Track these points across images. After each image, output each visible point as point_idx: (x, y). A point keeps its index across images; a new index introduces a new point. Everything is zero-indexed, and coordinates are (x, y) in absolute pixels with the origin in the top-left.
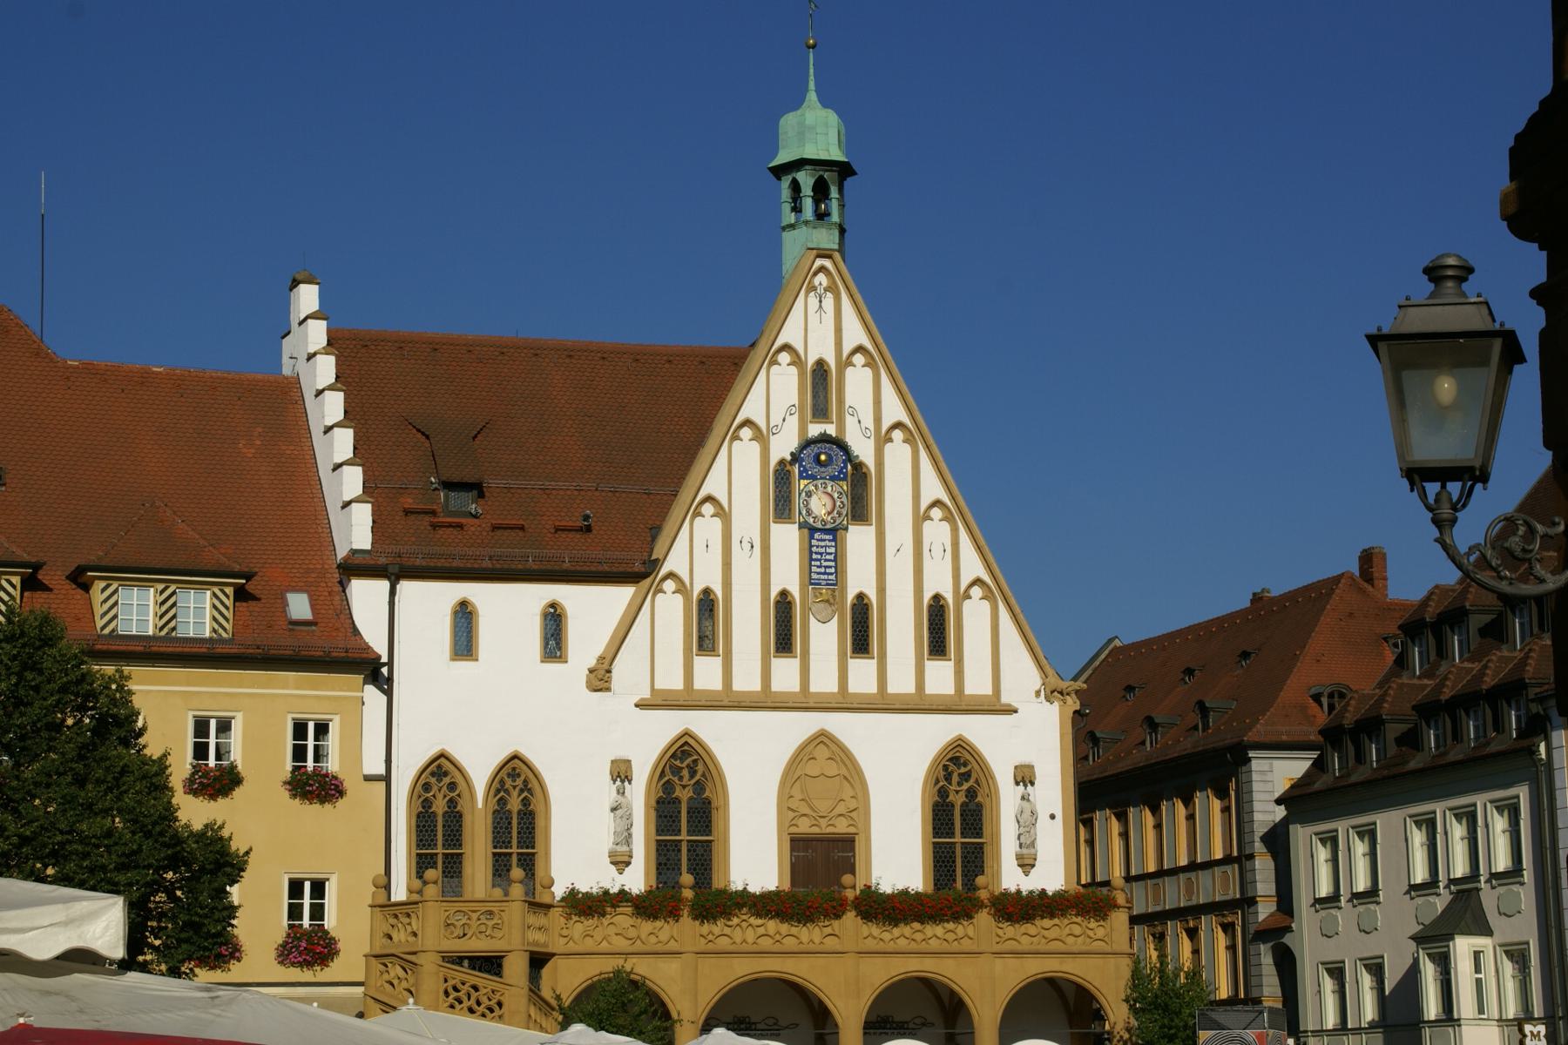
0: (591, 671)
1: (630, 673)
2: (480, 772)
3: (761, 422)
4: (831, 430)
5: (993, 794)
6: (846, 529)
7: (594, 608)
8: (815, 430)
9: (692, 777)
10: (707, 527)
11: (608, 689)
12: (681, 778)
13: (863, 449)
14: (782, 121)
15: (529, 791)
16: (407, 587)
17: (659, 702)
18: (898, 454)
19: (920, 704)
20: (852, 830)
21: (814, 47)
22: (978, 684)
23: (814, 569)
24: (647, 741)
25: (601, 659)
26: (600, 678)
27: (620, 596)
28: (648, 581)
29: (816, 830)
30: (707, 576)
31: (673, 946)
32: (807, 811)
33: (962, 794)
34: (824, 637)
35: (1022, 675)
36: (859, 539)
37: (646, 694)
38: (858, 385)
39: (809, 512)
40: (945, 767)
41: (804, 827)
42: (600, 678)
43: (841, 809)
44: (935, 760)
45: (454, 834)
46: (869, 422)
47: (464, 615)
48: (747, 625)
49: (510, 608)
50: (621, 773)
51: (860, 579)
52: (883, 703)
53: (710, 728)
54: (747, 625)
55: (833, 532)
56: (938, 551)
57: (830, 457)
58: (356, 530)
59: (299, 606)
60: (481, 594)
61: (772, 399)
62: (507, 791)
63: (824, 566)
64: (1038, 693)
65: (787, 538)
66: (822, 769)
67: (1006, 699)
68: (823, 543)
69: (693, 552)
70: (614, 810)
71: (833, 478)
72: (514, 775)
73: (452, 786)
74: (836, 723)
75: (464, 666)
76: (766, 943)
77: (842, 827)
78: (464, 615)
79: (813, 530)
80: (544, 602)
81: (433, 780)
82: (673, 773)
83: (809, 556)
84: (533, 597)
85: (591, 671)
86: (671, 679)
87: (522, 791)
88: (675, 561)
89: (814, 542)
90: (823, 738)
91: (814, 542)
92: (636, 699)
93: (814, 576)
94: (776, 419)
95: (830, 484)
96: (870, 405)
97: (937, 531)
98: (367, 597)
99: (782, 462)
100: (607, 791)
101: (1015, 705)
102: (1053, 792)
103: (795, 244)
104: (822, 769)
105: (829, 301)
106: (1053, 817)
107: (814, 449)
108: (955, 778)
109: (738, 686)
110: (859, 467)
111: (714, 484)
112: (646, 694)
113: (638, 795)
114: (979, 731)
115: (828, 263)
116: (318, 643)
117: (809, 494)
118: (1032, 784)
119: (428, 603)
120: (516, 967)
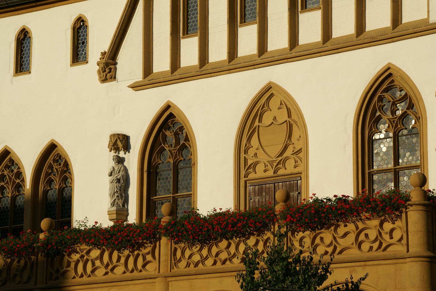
24: (137, 115)
26: (109, 68)
37: (139, 76)
47: (23, 39)
50: (121, 143)
60: (34, 20)
66: (268, 120)
75: (23, 78)
77: (290, 168)
78: (23, 39)
90: (268, 92)
92: (131, 82)
104: (268, 120)
113: (133, 161)
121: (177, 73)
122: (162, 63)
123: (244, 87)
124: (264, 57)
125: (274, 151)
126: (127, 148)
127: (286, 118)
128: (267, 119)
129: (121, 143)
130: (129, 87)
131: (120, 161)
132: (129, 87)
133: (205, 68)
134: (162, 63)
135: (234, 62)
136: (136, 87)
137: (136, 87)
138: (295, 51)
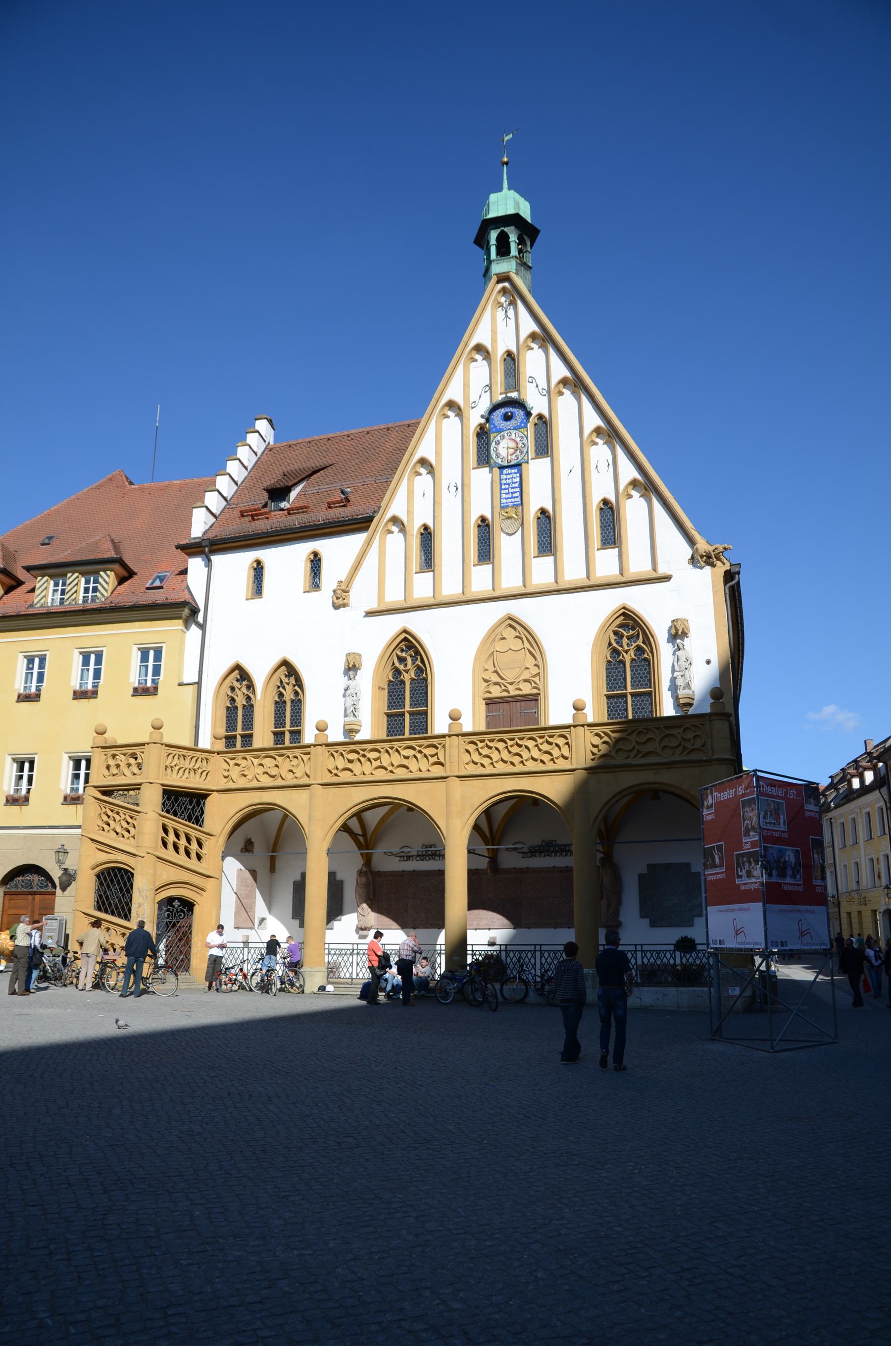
1: (363, 595)
3: (460, 401)
4: (514, 395)
6: (527, 462)
7: (338, 551)
8: (500, 398)
10: (424, 481)
13: (537, 404)
16: (216, 559)
18: (567, 402)
20: (535, 691)
22: (639, 564)
23: (503, 496)
27: (357, 540)
29: (505, 694)
30: (422, 516)
31: (305, 780)
32: (498, 680)
33: (632, 653)
34: (508, 547)
35: (674, 549)
36: (537, 471)
38: (534, 362)
39: (498, 456)
40: (616, 633)
41: (496, 692)
43: (526, 675)
44: (605, 628)
45: (249, 723)
46: (543, 384)
48: (451, 546)
51: (538, 497)
54: (451, 546)
55: (518, 465)
56: (603, 466)
61: (471, 384)
67: (662, 570)
69: (409, 499)
74: (521, 609)
76: (381, 775)
77: (527, 689)
79: (502, 468)
83: (497, 488)
86: (395, 595)
91: (503, 477)
93: (503, 501)
94: (473, 397)
95: (513, 432)
96: (540, 369)
97: (600, 452)
99: (482, 427)
101: (669, 573)
105: (511, 313)
106: (708, 662)
107: (502, 411)
108: (625, 640)
111: (425, 448)
112: (374, 606)
114: (638, 600)
115: (506, 284)
117: (498, 443)
119: (233, 566)
120: (151, 800)
136: (369, 614)
137: (369, 614)
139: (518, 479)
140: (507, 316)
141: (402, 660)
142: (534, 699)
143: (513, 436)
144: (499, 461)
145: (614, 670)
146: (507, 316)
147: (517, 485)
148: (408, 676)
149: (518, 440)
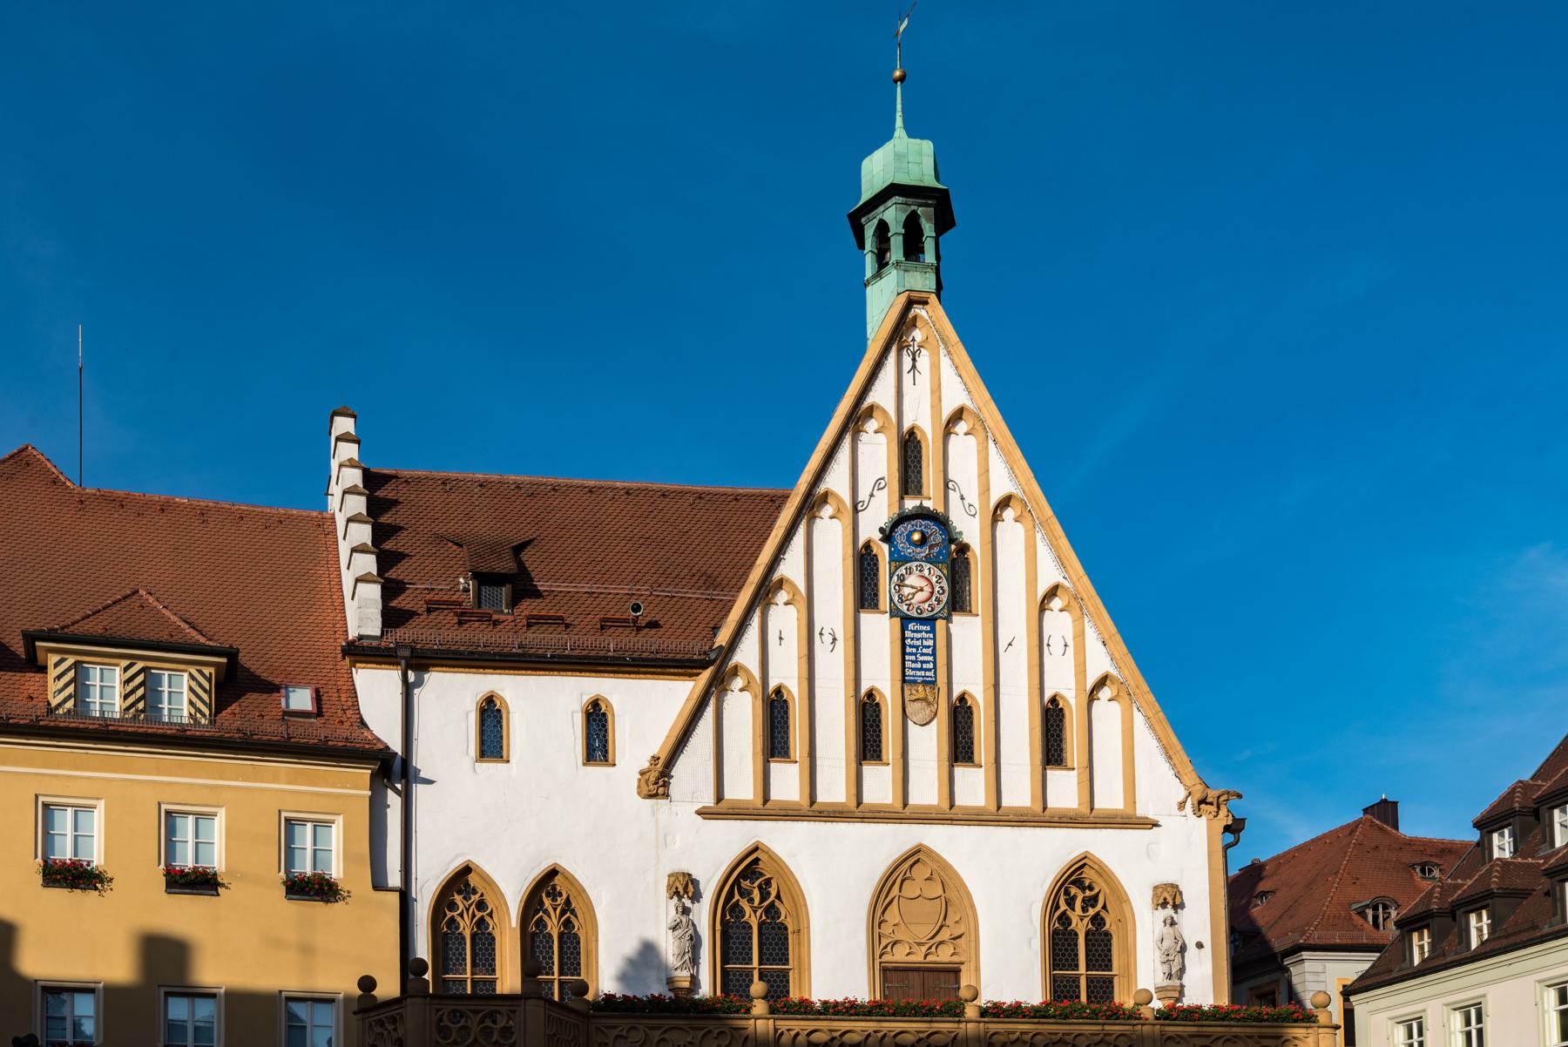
0: (642, 773)
2: (511, 887)
5: (1128, 920)
6: (948, 619)
7: (648, 707)
9: (763, 900)
11: (666, 795)
12: (751, 901)
14: (866, 164)
15: (573, 912)
17: (721, 810)
19: (1042, 817)
21: (902, 79)
22: (1109, 798)
23: (908, 664)
24: (713, 852)
25: (655, 759)
26: (658, 781)
27: (678, 693)
28: (706, 675)
35: (1161, 784)
37: (709, 800)
41: (899, 956)
42: (658, 781)
46: (973, 497)
49: (544, 705)
50: (684, 887)
52: (997, 816)
53: (789, 844)
55: (931, 621)
57: (924, 540)
58: (362, 612)
59: (301, 699)
60: (512, 688)
62: (546, 912)
63: (920, 670)
64: (1182, 805)
65: (879, 629)
67: (1141, 811)
68: (916, 632)
70: (674, 929)
71: (928, 559)
72: (554, 894)
73: (481, 905)
75: (491, 768)
80: (586, 698)
81: (458, 898)
82: (741, 895)
84: (573, 691)
85: (642, 773)
87: (563, 913)
88: (747, 655)
89: (908, 634)
92: (698, 806)
95: (927, 566)
98: (377, 691)
100: (667, 911)
102: (1202, 919)
103: (882, 302)
107: (909, 526)
109: (823, 797)
110: (964, 548)
113: (702, 914)
114: (1109, 849)
116: (316, 731)
118: (1178, 907)
119: (450, 698)
121: (765, 809)
122: (741, 787)
123: (894, 840)
124: (902, 813)
125: (924, 932)
126: (696, 897)
127: (940, 892)
128: (910, 890)
129: (684, 887)
130: (699, 813)
131: (686, 911)
132: (699, 813)
133: (813, 811)
134: (741, 787)
135: (857, 812)
136: (704, 813)
137: (704, 813)
138: (950, 814)
139: (931, 643)
140: (914, 367)
141: (746, 894)
142: (955, 972)
143: (926, 572)
144: (904, 608)
145: (1059, 946)
146: (914, 367)
147: (929, 651)
148: (754, 917)
149: (934, 580)
